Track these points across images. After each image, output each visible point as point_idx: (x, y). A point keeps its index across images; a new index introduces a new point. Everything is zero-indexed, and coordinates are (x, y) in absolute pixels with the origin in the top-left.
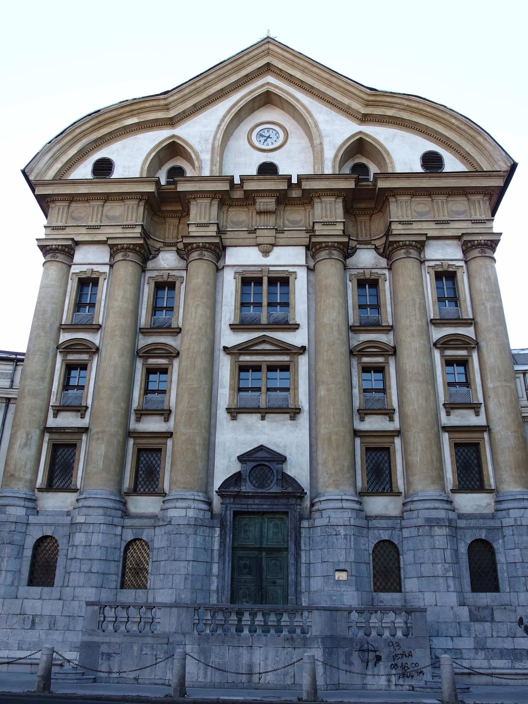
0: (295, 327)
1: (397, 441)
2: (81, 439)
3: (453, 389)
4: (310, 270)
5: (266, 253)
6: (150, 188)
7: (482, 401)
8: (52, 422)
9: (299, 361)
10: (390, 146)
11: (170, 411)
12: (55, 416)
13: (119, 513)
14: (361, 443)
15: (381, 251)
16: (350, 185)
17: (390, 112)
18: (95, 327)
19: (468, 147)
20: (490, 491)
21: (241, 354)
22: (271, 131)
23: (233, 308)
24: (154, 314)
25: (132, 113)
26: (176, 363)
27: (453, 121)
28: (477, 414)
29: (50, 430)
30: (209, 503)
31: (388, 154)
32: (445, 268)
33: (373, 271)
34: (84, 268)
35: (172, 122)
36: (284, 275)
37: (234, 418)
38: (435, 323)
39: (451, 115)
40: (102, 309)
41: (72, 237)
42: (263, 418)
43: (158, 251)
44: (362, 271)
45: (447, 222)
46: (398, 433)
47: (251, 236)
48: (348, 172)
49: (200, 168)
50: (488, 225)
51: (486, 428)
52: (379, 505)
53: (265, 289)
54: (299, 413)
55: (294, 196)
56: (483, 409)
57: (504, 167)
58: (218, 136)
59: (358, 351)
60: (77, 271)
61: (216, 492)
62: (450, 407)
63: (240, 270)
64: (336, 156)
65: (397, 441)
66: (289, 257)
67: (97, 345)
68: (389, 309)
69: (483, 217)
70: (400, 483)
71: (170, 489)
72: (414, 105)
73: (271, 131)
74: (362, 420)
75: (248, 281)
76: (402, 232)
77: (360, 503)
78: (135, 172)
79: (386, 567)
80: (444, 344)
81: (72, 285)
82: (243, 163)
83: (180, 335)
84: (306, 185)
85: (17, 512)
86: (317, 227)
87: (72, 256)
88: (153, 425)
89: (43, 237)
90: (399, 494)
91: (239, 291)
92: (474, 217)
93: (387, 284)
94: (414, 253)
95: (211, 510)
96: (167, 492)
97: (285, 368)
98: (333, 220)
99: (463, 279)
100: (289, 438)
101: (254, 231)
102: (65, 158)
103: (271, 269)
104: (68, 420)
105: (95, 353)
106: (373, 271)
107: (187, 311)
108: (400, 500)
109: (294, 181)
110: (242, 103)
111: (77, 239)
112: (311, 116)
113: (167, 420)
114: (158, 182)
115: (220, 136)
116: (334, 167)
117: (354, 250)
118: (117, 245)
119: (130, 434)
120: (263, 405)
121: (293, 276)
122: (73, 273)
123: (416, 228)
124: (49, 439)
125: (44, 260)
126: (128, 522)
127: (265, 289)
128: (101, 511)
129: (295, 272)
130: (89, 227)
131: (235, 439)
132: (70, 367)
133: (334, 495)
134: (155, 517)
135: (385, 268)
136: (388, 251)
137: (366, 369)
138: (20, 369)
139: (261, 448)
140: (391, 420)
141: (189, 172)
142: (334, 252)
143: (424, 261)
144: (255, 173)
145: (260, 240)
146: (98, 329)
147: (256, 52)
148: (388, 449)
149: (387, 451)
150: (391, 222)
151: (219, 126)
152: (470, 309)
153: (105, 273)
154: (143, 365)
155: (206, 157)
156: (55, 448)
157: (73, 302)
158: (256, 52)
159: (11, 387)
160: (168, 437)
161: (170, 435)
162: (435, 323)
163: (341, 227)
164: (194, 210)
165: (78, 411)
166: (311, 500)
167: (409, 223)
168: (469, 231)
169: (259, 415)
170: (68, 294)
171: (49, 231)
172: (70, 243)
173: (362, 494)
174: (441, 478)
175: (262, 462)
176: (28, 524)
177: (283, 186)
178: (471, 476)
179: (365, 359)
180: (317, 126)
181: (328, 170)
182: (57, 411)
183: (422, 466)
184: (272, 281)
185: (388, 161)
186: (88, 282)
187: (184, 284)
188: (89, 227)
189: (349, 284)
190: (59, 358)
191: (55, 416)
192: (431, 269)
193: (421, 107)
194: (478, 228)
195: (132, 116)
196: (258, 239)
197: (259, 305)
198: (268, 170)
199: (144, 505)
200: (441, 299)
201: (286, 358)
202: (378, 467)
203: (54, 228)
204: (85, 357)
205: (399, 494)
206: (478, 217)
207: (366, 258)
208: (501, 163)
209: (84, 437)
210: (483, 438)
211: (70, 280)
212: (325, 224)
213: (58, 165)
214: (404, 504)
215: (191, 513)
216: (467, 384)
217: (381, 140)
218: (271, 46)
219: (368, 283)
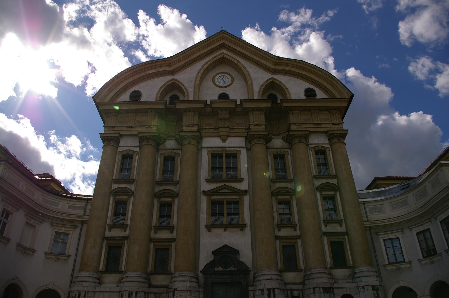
0: (241, 180)
1: (299, 241)
2: (124, 243)
3: (327, 212)
4: (248, 150)
5: (224, 141)
6: (162, 106)
7: (343, 218)
8: (108, 234)
9: (244, 198)
10: (288, 85)
11: (174, 227)
12: (110, 230)
13: (147, 285)
14: (279, 243)
15: (285, 139)
16: (268, 105)
17: (287, 68)
18: (132, 181)
19: (328, 86)
20: (350, 267)
21: (212, 195)
22: (225, 77)
23: (207, 170)
24: (163, 174)
25: (151, 68)
26: (176, 200)
27: (320, 73)
28: (341, 226)
29: (107, 238)
30: (197, 278)
31: (287, 89)
32: (320, 148)
33: (282, 150)
34: (125, 149)
35: (172, 73)
36: (234, 152)
37: (209, 230)
38: (316, 177)
39: (319, 70)
40: (135, 171)
41: (119, 132)
42: (225, 230)
43: (165, 140)
44: (276, 150)
45: (319, 124)
46: (299, 237)
47: (216, 131)
48: (266, 98)
49: (188, 95)
50: (341, 126)
51: (346, 233)
52: (290, 276)
54: (245, 227)
55: (239, 110)
56: (344, 222)
57: (347, 96)
58: (197, 79)
59: (276, 193)
60: (121, 150)
61: (201, 271)
62: (327, 222)
63: (210, 149)
64: (260, 90)
65: (299, 241)
66: (236, 143)
67: (133, 190)
68: (291, 170)
69: (338, 122)
70: (302, 265)
71: (175, 272)
72: (299, 65)
73: (225, 77)
74: (279, 230)
75: (215, 156)
76: (296, 129)
77: (281, 276)
78: (153, 98)
80: (321, 188)
81: (119, 159)
82: (210, 93)
83: (178, 186)
84: (245, 105)
86: (251, 127)
87: (118, 142)
88: (164, 235)
89: (103, 132)
90: (301, 270)
91: (210, 161)
92: (333, 122)
93: (289, 157)
94: (303, 140)
95: (198, 282)
96: (173, 272)
97: (237, 202)
98: (260, 123)
99: (330, 154)
100: (240, 241)
101: (218, 129)
102: (115, 91)
103: (227, 149)
104: (117, 233)
105: (132, 195)
106: (282, 150)
107: (182, 172)
108: (302, 274)
109: (239, 103)
110: (209, 63)
111: (122, 133)
112: (246, 70)
113: (172, 232)
114: (166, 103)
115: (198, 79)
116: (259, 95)
117: (271, 139)
118: (143, 136)
119: (151, 240)
120: (225, 222)
121: (239, 152)
122: (119, 152)
123: (304, 127)
124: (106, 243)
125: (103, 145)
126: (152, 290)
128: (137, 283)
129: (240, 151)
130: (128, 127)
131: (210, 242)
132: (118, 203)
134: (167, 286)
135: (288, 148)
136: (290, 139)
137: (280, 203)
138: (89, 205)
139: (225, 246)
140: (295, 230)
141: (182, 98)
142: (261, 140)
143: (309, 144)
144: (217, 99)
145: (221, 134)
146: (133, 182)
147: (217, 37)
148: (294, 246)
149: (294, 247)
150: (290, 124)
151: (198, 74)
152: (334, 170)
153: (137, 151)
154: (158, 201)
155: (191, 90)
156: (110, 248)
157: (119, 167)
158: (217, 37)
159: (84, 214)
160: (172, 242)
161: (174, 240)
162: (316, 177)
163: (264, 127)
164: (185, 119)
165: (122, 227)
166: (254, 275)
167: (300, 125)
168: (331, 129)
169: (223, 229)
170: (116, 163)
171: (106, 129)
172: (118, 135)
173: (281, 271)
174: (324, 260)
175: (226, 254)
176: (95, 292)
177: (233, 105)
179: (280, 197)
180: (249, 75)
181: (256, 97)
182: (111, 227)
184: (228, 156)
185: (287, 93)
186: (127, 157)
187: (180, 157)
188: (128, 127)
189: (269, 157)
190: (112, 198)
191: (110, 230)
192: (312, 149)
193: (303, 66)
194: (336, 127)
195: (152, 69)
196: (220, 133)
197: (221, 169)
198: (224, 97)
199: (160, 280)
200: (318, 165)
201: (237, 197)
203: (109, 127)
204: (126, 197)
205: (301, 270)
206: (335, 122)
207: (277, 143)
208: (346, 95)
209: (126, 242)
210: (345, 238)
211: (117, 156)
212: (255, 125)
213: (112, 94)
214: (304, 276)
215: (188, 284)
216: (335, 209)
217: (283, 82)
218: (224, 35)
219: (279, 157)
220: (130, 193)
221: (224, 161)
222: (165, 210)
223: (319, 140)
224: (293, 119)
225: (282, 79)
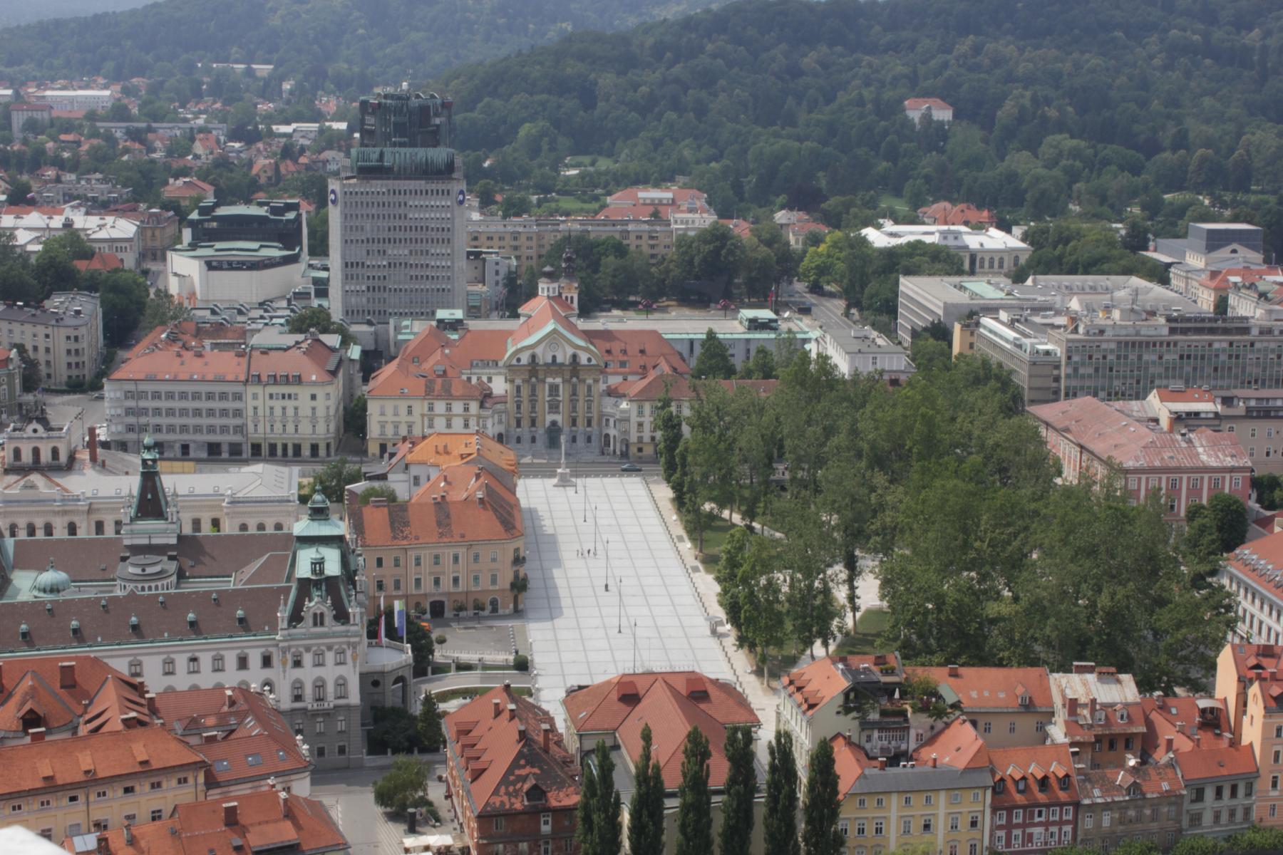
53: (554, 389)
79: (574, 440)
100: (558, 418)
107: (539, 392)
133: (566, 429)
175: (554, 423)
178: (589, 424)
183: (581, 422)
202: (574, 422)
221: (554, 389)
222: (533, 407)
223: (590, 381)
225: (579, 352)
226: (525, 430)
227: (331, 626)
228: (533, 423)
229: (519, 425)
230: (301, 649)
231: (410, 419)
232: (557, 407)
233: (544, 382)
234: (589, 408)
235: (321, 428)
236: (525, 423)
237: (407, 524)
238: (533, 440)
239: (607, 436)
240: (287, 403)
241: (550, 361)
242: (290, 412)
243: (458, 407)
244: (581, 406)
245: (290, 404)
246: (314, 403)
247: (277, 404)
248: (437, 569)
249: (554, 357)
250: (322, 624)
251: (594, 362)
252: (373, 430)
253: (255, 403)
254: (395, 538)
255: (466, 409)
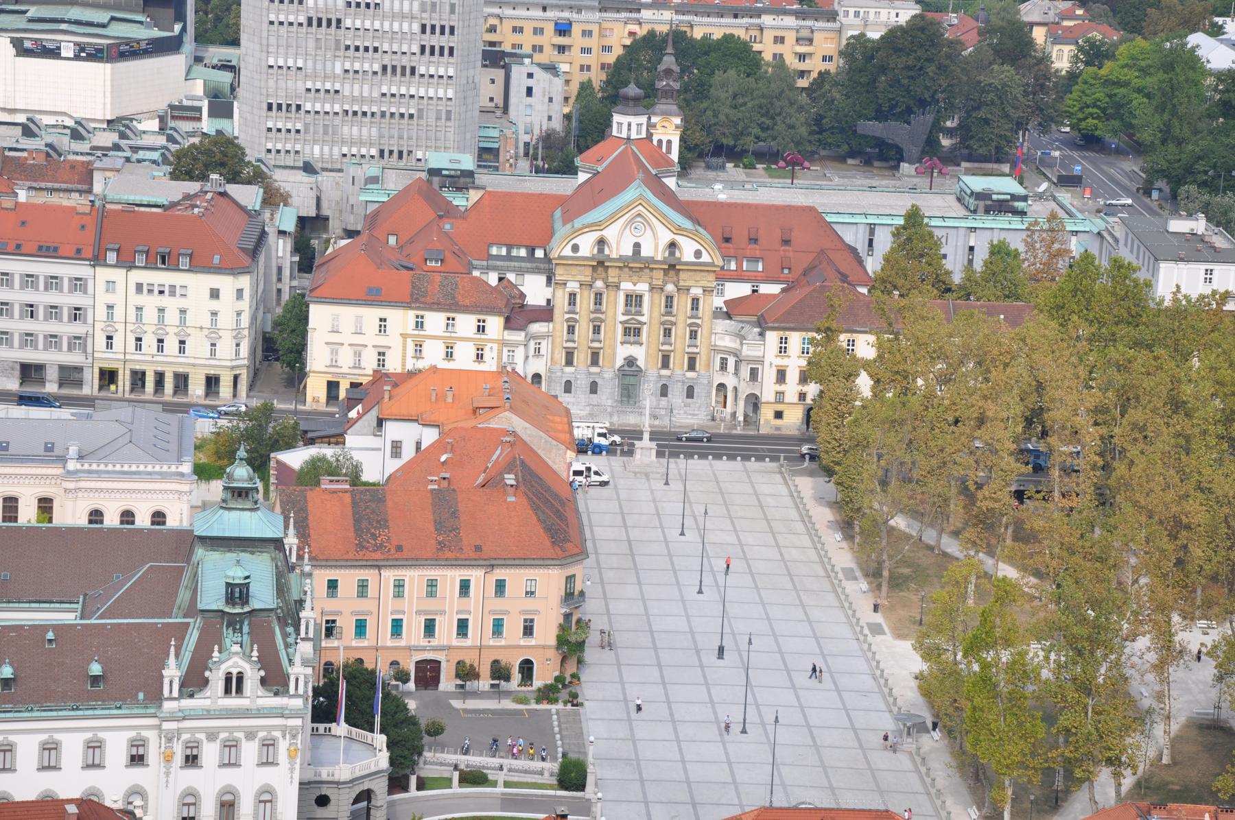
66: (642, 287)
79: (664, 391)
80: (690, 325)
81: (567, 297)
85: (559, 374)
88: (596, 345)
100: (639, 353)
104: (570, 345)
127: (633, 300)
181: (659, 258)
199: (595, 369)
207: (670, 288)
220: (576, 321)
221: (633, 300)
222: (597, 330)
223: (696, 291)
224: (682, 275)
225: (680, 240)
226: (580, 372)
227: (254, 695)
228: (595, 359)
229: (569, 362)
230: (240, 735)
231: (382, 341)
232: (638, 332)
233: (618, 287)
234: (693, 335)
235: (226, 349)
236: (582, 358)
237: (383, 523)
238: (594, 388)
239: (722, 386)
240: (165, 301)
241: (628, 251)
242: (172, 317)
243: (466, 323)
244: (680, 332)
245: (172, 305)
246: (214, 305)
247: (151, 303)
248: (431, 604)
249: (637, 246)
250: (239, 690)
251: (705, 258)
252: (317, 357)
253: (110, 298)
254: (361, 546)
255: (481, 329)
